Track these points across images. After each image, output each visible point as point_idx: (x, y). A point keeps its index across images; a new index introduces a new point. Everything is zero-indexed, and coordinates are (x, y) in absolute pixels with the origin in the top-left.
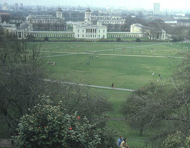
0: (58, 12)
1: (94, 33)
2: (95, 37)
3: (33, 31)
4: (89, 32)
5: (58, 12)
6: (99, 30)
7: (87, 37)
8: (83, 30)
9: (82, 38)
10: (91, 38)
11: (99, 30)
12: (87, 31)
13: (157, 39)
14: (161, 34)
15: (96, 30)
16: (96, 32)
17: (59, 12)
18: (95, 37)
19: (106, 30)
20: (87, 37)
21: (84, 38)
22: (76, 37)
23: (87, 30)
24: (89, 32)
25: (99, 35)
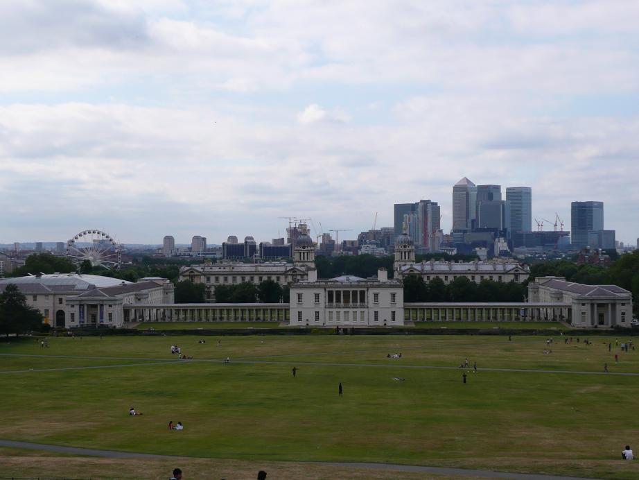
0: (299, 248)
1: (359, 303)
2: (362, 318)
3: (175, 303)
4: (338, 300)
5: (299, 248)
6: (376, 295)
7: (331, 318)
8: (317, 296)
9: (313, 323)
10: (347, 323)
11: (376, 295)
12: (330, 300)
13: (599, 326)
14: (614, 305)
15: (362, 293)
16: (362, 300)
17: (304, 247)
18: (362, 318)
19: (400, 293)
20: (331, 318)
21: (320, 323)
22: (294, 322)
23: (330, 295)
24: (338, 300)
25: (376, 313)
